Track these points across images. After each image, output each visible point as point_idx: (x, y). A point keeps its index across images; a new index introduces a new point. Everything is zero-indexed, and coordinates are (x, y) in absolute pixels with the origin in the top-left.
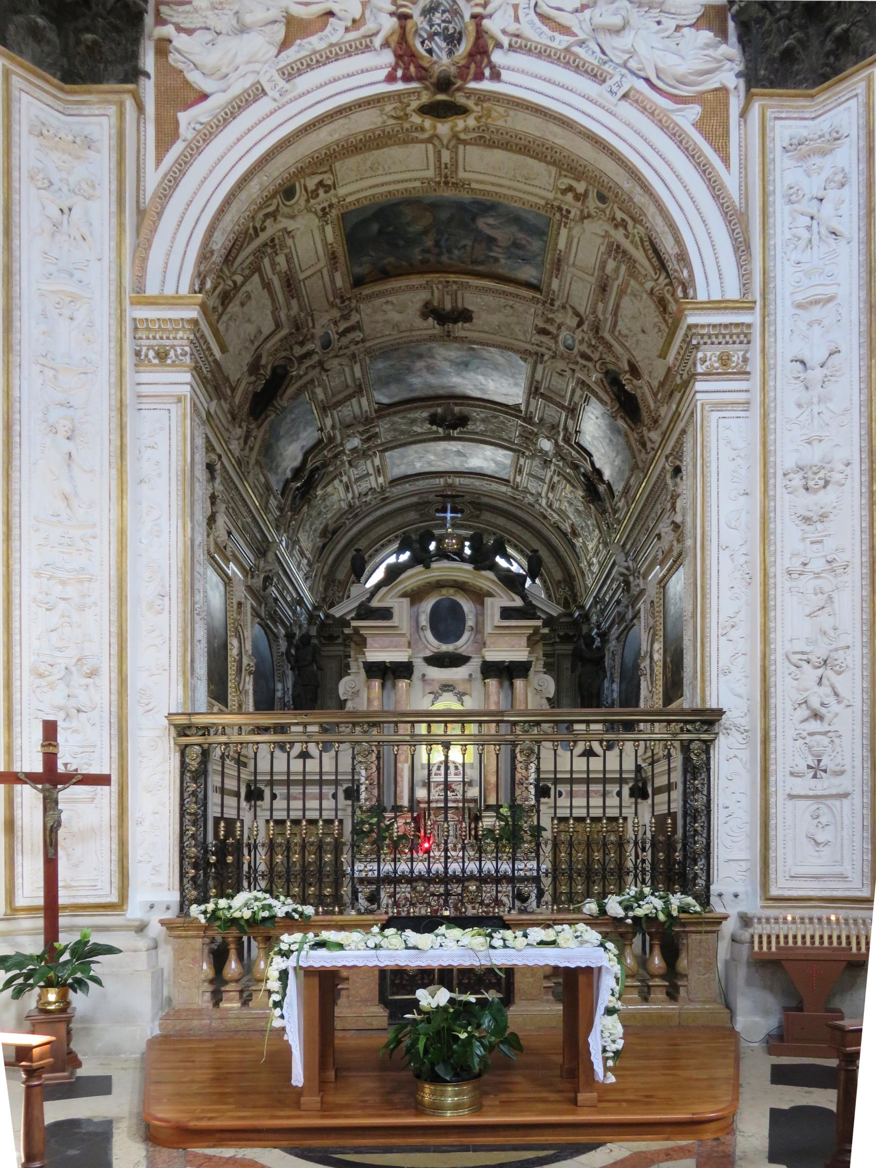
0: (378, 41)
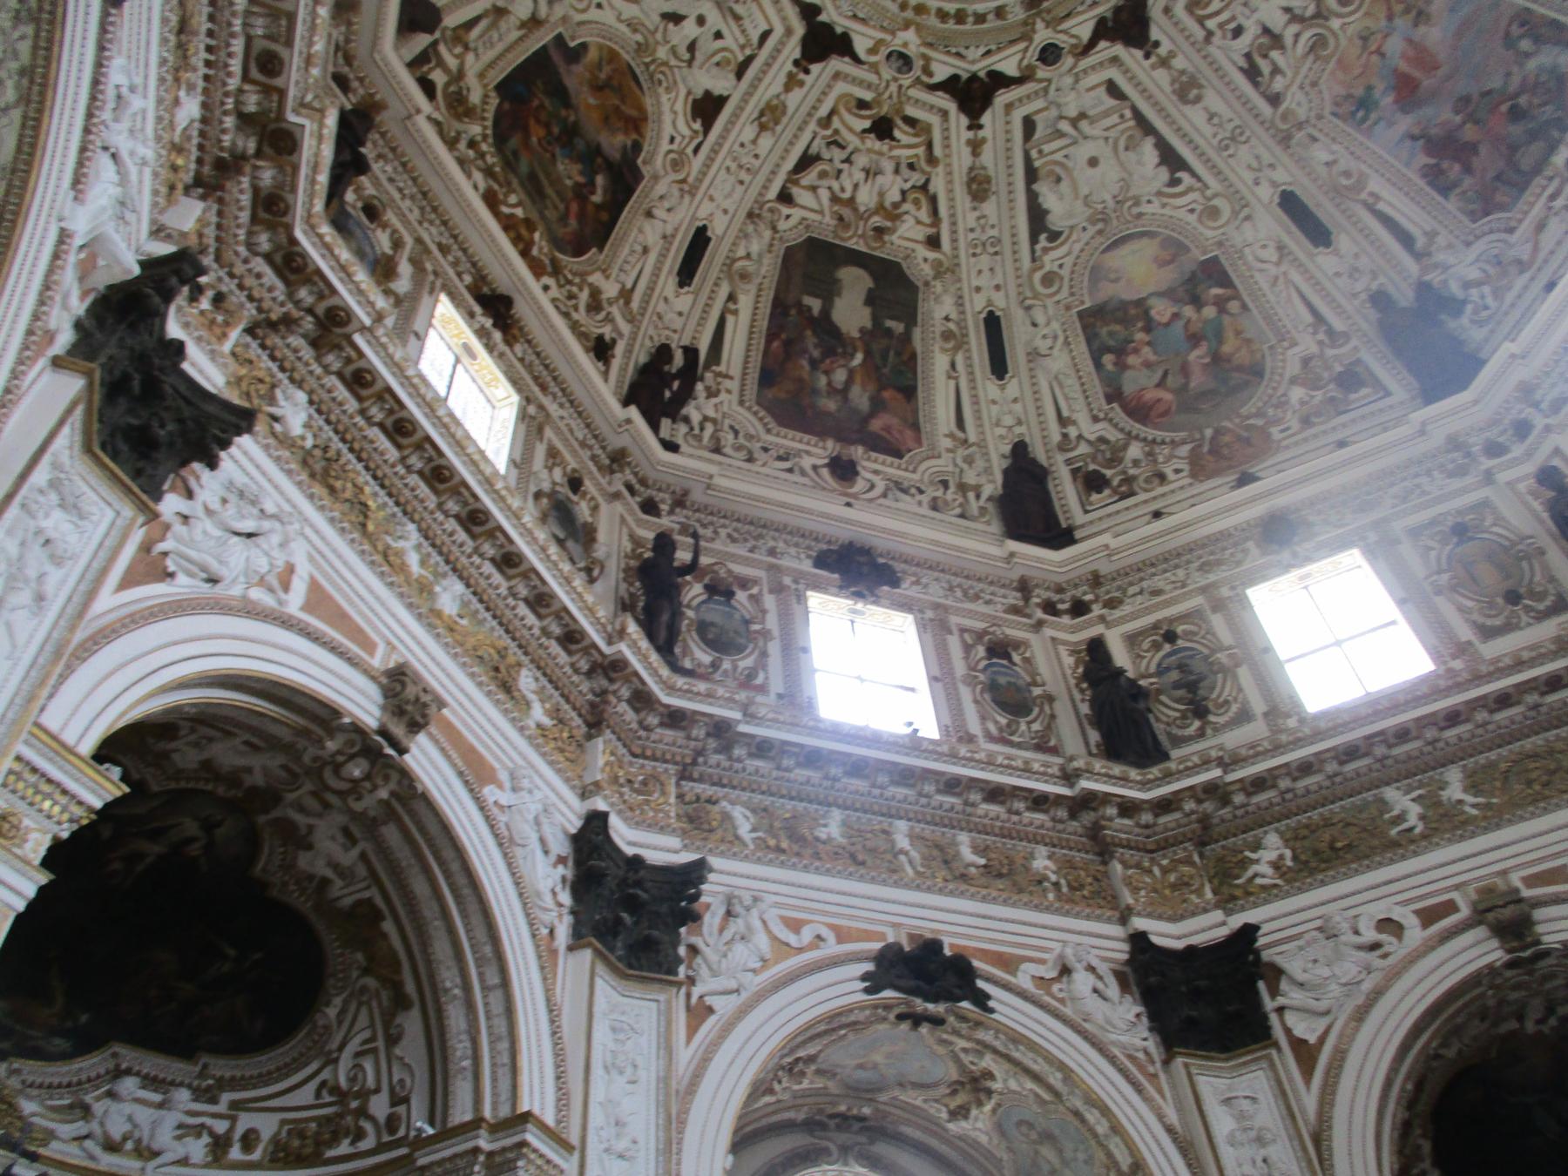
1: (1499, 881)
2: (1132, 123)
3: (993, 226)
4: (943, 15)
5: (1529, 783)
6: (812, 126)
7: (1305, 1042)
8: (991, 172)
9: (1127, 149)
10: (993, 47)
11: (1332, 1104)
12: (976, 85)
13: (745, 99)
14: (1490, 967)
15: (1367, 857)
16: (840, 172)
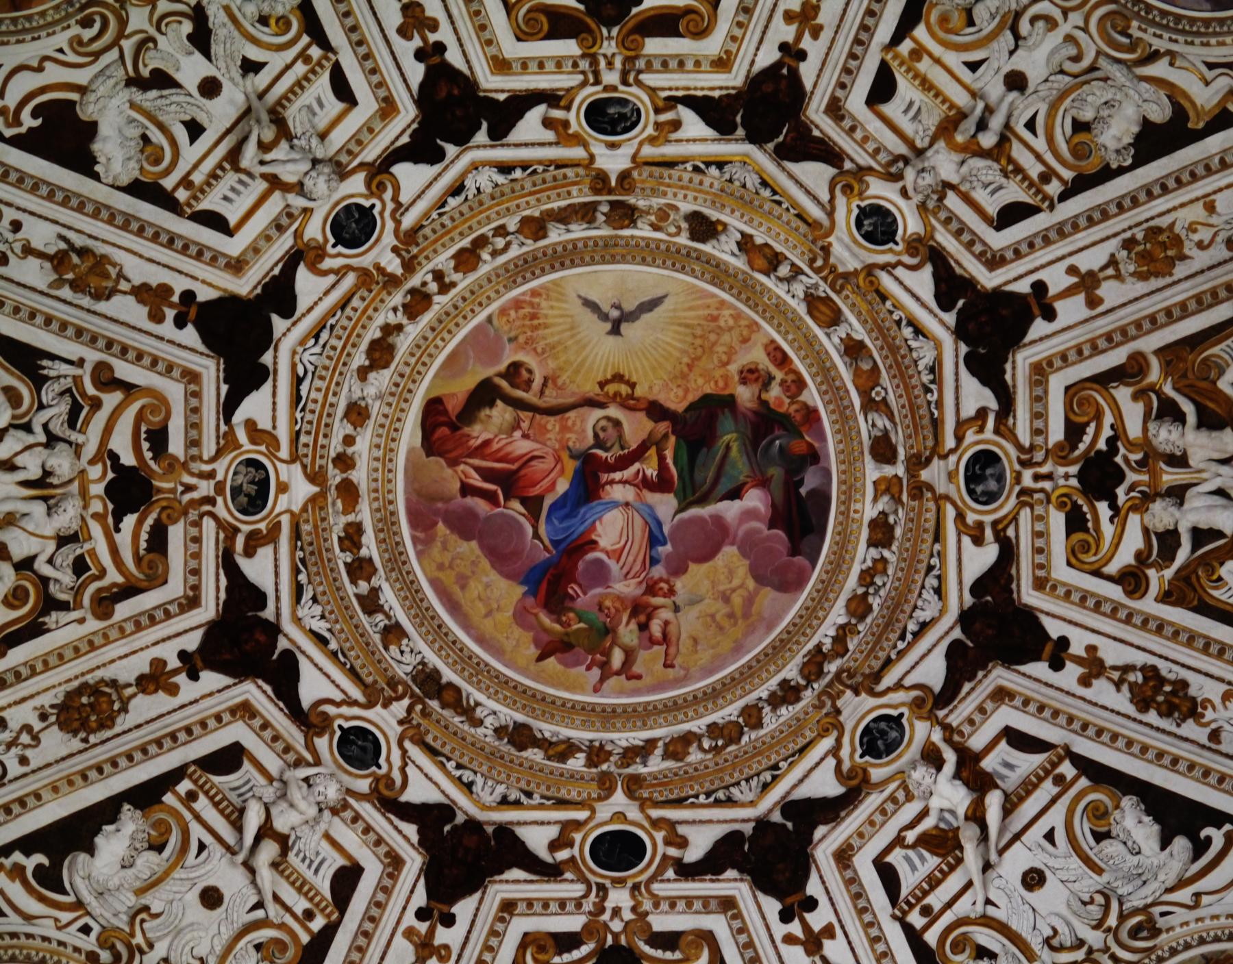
2: (305, 938)
3: (23, 761)
4: (353, 536)
6: (93, 356)
8: (123, 722)
9: (258, 947)
10: (333, 645)
12: (261, 638)
13: (97, 211)
16: (27, 428)
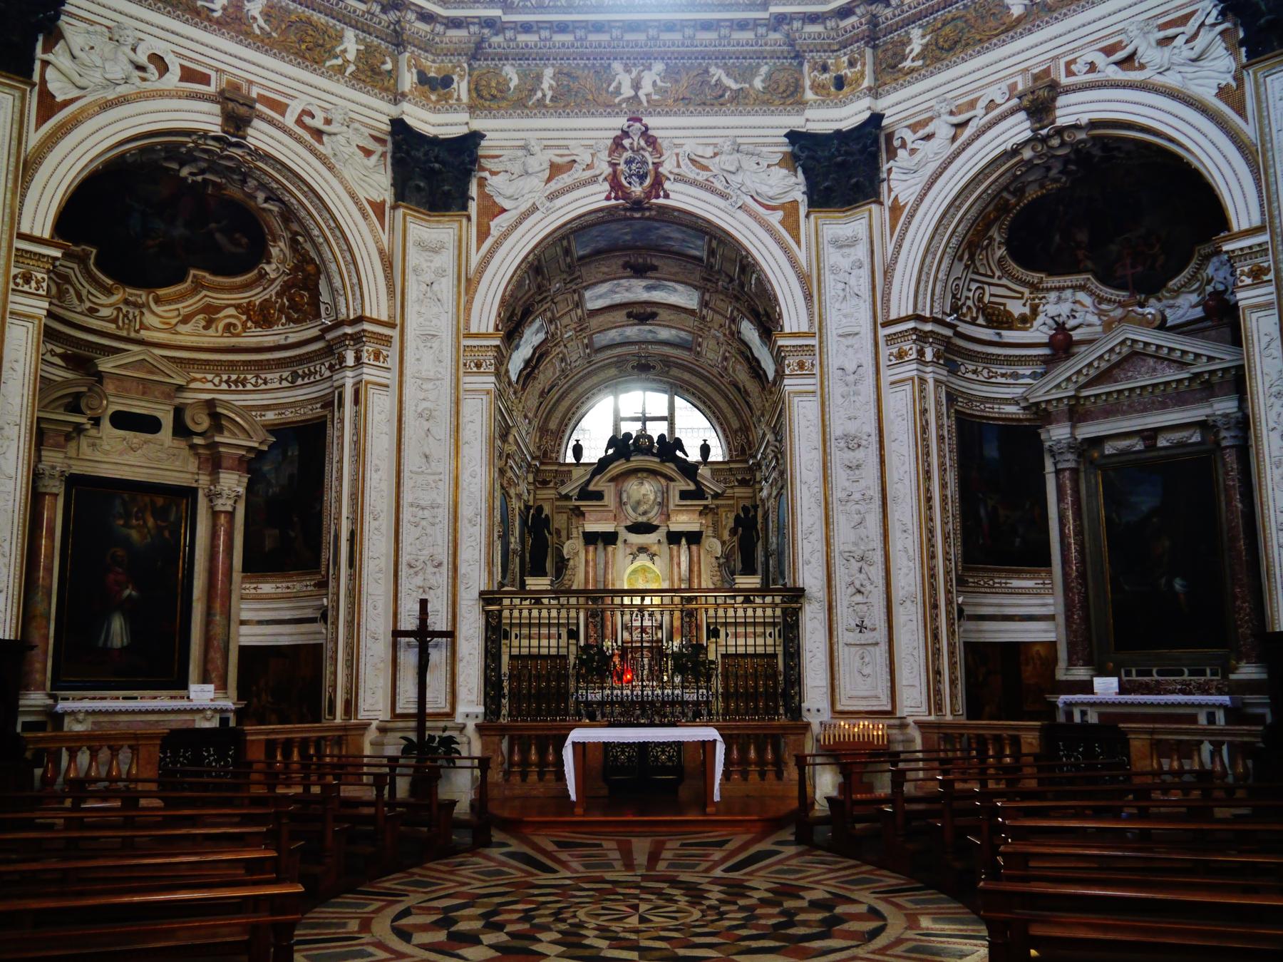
0: (601, 179)
1: (245, 86)
5: (302, 41)
7: (53, 97)
11: (50, 149)
14: (205, 135)
15: (172, 6)
